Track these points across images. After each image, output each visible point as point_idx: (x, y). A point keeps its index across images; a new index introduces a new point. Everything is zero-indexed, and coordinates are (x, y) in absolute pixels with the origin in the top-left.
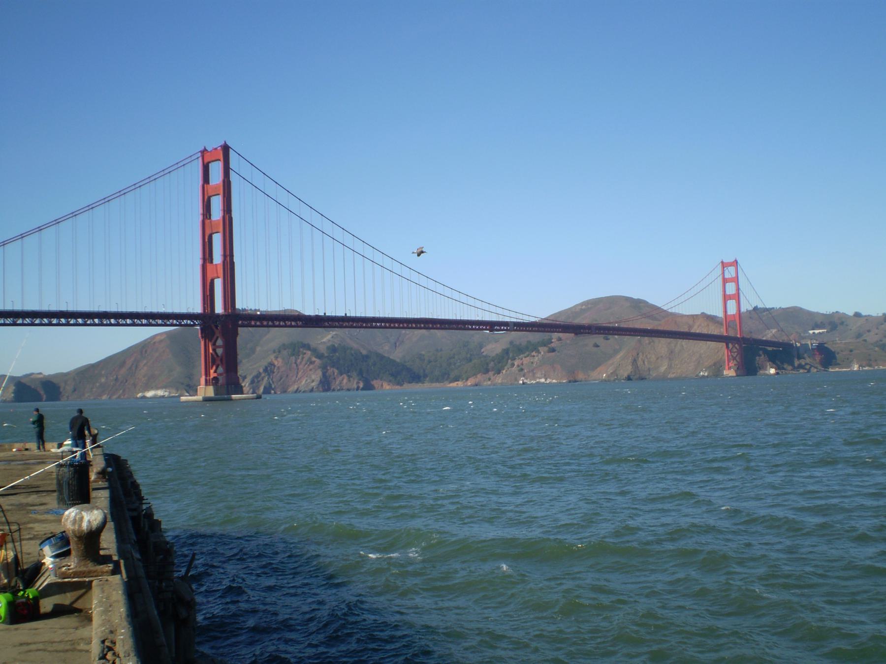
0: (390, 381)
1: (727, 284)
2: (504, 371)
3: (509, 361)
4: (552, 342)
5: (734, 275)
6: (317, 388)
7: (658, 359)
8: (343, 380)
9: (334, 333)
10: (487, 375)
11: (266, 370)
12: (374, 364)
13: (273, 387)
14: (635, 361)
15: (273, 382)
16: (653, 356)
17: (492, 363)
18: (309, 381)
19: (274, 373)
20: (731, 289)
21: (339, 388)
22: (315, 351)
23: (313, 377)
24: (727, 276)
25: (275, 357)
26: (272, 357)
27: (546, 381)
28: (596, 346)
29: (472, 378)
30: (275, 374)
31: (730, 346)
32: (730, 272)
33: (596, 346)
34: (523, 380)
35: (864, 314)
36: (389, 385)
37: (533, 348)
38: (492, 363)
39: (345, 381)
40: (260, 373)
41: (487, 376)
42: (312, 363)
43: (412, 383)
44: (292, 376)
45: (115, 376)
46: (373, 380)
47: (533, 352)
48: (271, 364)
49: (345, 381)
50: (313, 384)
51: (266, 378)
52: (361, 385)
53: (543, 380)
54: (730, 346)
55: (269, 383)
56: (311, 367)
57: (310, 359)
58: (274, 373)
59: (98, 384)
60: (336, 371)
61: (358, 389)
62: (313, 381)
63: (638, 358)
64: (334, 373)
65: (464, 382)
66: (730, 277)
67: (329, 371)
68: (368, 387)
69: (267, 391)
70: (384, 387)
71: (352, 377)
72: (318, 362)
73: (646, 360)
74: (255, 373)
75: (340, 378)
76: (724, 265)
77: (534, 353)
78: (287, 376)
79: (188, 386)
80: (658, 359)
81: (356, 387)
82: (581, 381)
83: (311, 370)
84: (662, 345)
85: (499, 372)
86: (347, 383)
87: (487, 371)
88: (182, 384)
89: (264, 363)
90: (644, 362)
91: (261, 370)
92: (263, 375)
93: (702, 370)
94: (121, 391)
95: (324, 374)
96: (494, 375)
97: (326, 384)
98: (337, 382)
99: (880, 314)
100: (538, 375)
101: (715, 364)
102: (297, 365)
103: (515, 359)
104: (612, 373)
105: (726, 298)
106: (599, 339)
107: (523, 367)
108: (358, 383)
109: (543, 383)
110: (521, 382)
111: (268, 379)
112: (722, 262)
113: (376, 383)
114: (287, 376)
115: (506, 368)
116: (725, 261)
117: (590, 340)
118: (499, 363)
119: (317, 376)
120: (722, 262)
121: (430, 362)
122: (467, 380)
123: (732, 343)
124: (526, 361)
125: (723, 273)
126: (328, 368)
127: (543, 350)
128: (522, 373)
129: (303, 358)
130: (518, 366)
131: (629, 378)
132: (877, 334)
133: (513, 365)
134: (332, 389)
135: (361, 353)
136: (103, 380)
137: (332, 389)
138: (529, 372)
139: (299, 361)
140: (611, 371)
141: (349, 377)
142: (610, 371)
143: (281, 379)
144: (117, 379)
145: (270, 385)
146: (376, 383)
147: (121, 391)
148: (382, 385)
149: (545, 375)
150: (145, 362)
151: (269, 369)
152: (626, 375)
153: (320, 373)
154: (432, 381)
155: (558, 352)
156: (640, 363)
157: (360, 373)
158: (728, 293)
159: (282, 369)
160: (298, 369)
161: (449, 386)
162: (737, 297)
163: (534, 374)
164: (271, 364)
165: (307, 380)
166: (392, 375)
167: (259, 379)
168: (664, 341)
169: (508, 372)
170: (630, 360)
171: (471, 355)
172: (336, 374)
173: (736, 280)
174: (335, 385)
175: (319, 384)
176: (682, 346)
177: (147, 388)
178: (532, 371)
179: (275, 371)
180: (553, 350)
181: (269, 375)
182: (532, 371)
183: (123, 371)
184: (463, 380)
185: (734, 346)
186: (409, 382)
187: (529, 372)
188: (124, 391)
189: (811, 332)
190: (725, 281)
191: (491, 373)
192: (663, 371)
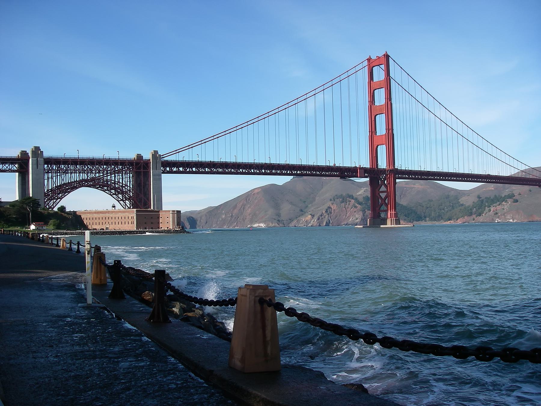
0: (405, 220)
2: (484, 214)
3: (486, 207)
4: (515, 196)
11: (326, 211)
13: (331, 222)
17: (475, 209)
22: (356, 199)
23: (357, 216)
27: (513, 221)
34: (498, 220)
37: (498, 199)
38: (475, 209)
41: (472, 218)
42: (356, 207)
44: (343, 215)
47: (502, 202)
48: (329, 208)
50: (357, 221)
51: (327, 217)
53: (511, 221)
55: (329, 219)
56: (355, 210)
57: (354, 205)
58: (331, 213)
62: (357, 219)
65: (455, 221)
69: (327, 224)
72: (359, 206)
77: (504, 203)
83: (355, 212)
85: (480, 215)
87: (471, 214)
89: (326, 207)
91: (324, 212)
92: (325, 214)
102: (346, 209)
103: (490, 206)
110: (497, 221)
115: (485, 212)
118: (479, 209)
124: (499, 208)
126: (366, 210)
127: (510, 201)
129: (349, 204)
130: (494, 211)
133: (490, 210)
136: (223, 217)
139: (347, 206)
149: (512, 218)
153: (361, 213)
154: (431, 220)
155: (520, 202)
159: (337, 211)
163: (505, 216)
164: (329, 208)
167: (322, 217)
169: (487, 215)
171: (453, 204)
177: (252, 221)
178: (504, 214)
180: (516, 201)
182: (504, 214)
183: (236, 211)
187: (501, 215)
191: (474, 216)
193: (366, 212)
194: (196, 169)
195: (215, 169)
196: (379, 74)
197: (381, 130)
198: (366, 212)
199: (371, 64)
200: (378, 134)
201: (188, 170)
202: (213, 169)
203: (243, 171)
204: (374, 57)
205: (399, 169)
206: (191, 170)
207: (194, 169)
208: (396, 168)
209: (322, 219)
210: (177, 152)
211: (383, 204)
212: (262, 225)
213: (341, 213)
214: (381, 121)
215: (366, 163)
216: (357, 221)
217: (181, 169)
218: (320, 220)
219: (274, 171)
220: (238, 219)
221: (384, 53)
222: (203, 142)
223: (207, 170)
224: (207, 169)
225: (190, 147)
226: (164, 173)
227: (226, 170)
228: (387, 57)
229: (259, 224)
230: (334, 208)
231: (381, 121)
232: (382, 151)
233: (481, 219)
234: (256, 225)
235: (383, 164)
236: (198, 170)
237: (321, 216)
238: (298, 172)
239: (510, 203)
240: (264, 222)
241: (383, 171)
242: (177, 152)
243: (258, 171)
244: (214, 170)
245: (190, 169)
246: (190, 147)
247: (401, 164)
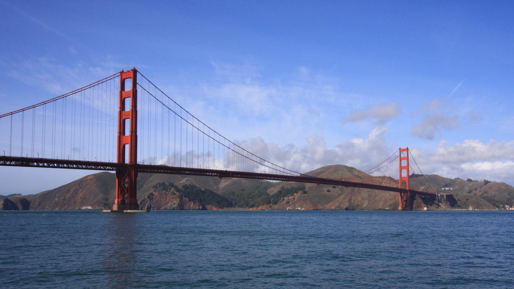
0: (216, 206)
3: (282, 197)
6: (176, 208)
7: (362, 199)
8: (191, 204)
9: (187, 179)
10: (269, 205)
11: (149, 197)
12: (208, 196)
13: (152, 206)
14: (350, 200)
15: (152, 204)
16: (360, 198)
18: (172, 204)
19: (153, 199)
21: (188, 208)
23: (175, 202)
25: (154, 190)
26: (152, 191)
27: (301, 209)
28: (329, 191)
29: (261, 206)
30: (154, 199)
31: (403, 194)
33: (329, 191)
34: (289, 208)
36: (215, 208)
39: (192, 205)
40: (145, 199)
43: (228, 207)
44: (163, 201)
45: (64, 198)
46: (207, 205)
47: (295, 193)
49: (192, 205)
50: (175, 206)
51: (149, 202)
52: (201, 208)
53: (299, 208)
54: (403, 194)
55: (150, 204)
56: (174, 196)
58: (153, 199)
59: (53, 202)
60: (187, 199)
61: (199, 209)
62: (175, 204)
63: (352, 198)
64: (186, 200)
67: (183, 199)
68: (204, 208)
70: (213, 209)
71: (196, 203)
72: (178, 194)
73: (356, 200)
74: (142, 199)
75: (190, 203)
78: (160, 201)
79: (105, 204)
80: (362, 199)
81: (198, 208)
82: (320, 210)
83: (173, 198)
84: (365, 192)
85: (276, 203)
86: (193, 206)
87: (269, 202)
88: (102, 203)
89: (148, 193)
90: (355, 201)
91: (146, 197)
92: (147, 200)
93: (387, 207)
94: (67, 206)
95: (180, 201)
96: (273, 205)
97: (181, 207)
98: (188, 205)
99: (483, 181)
100: (297, 206)
101: (394, 204)
102: (166, 195)
103: (285, 197)
104: (337, 206)
106: (330, 187)
107: (289, 201)
108: (199, 206)
109: (300, 210)
110: (288, 209)
111: (150, 202)
113: (208, 207)
114: (160, 201)
115: (280, 201)
117: (325, 188)
119: (176, 202)
121: (238, 196)
122: (258, 207)
123: (404, 193)
124: (291, 198)
126: (183, 197)
128: (288, 204)
131: (346, 209)
132: (480, 191)
133: (284, 200)
134: (185, 209)
135: (201, 190)
136: (57, 199)
137: (185, 209)
138: (292, 204)
140: (337, 205)
141: (194, 203)
142: (337, 204)
143: (157, 202)
144: (64, 199)
145: (151, 206)
146: (208, 207)
147: (67, 206)
148: (212, 208)
150: (81, 190)
151: (151, 197)
152: (345, 207)
153: (178, 200)
154: (239, 206)
156: (352, 201)
157: (201, 201)
159: (158, 197)
160: (166, 197)
161: (248, 209)
163: (295, 205)
164: (152, 194)
165: (171, 204)
166: (218, 202)
167: (145, 202)
168: (365, 190)
169: (281, 203)
170: (348, 199)
172: (187, 201)
174: (187, 206)
175: (177, 206)
176: (376, 193)
177: (82, 204)
178: (294, 203)
179: (154, 197)
181: (150, 200)
182: (294, 203)
183: (69, 195)
184: (256, 207)
185: (404, 194)
186: (227, 207)
187: (292, 204)
188: (68, 206)
189: (443, 189)
191: (271, 204)
192: (364, 206)
193: (183, 199)
198: (183, 199)
201: (51, 165)
203: (109, 168)
206: (63, 166)
207: (65, 165)
209: (144, 203)
212: (90, 208)
213: (162, 199)
216: (175, 206)
218: (142, 205)
220: (70, 202)
223: (74, 167)
224: (74, 165)
229: (87, 207)
230: (155, 194)
233: (276, 207)
234: (84, 208)
236: (68, 166)
237: (144, 201)
238: (149, 170)
239: (300, 194)
240: (91, 205)
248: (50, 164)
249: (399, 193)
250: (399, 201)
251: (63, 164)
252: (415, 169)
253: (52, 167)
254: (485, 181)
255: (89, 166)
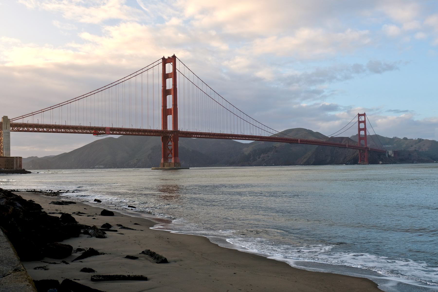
1: (360, 124)
5: (363, 119)
20: (362, 126)
24: (360, 120)
31: (361, 151)
32: (362, 118)
35: (408, 138)
66: (361, 121)
76: (359, 115)
105: (360, 130)
112: (358, 114)
116: (359, 114)
120: (358, 114)
125: (359, 119)
158: (360, 128)
162: (365, 129)
173: (364, 122)
190: (360, 122)
192: (328, 162)
194: (55, 130)
195: (68, 130)
196: (169, 68)
197: (170, 105)
199: (165, 61)
200: (168, 108)
202: (67, 130)
204: (166, 57)
205: (181, 130)
207: (54, 130)
208: (178, 130)
210: (23, 117)
211: (169, 153)
214: (170, 98)
215: (159, 127)
217: (45, 129)
219: (115, 132)
221: (173, 55)
222: (42, 111)
223: (63, 131)
224: (63, 130)
225: (33, 114)
226: (13, 130)
227: (76, 130)
228: (174, 57)
231: (170, 98)
232: (170, 118)
235: (170, 127)
238: (130, 133)
241: (171, 132)
242: (23, 117)
243: (105, 132)
244: (67, 130)
245: (51, 129)
246: (33, 114)
247: (181, 127)
248: (49, 129)
249: (358, 150)
250: (359, 156)
251: (61, 129)
252: (370, 132)
253: (50, 132)
254: (418, 139)
255: (76, 130)
